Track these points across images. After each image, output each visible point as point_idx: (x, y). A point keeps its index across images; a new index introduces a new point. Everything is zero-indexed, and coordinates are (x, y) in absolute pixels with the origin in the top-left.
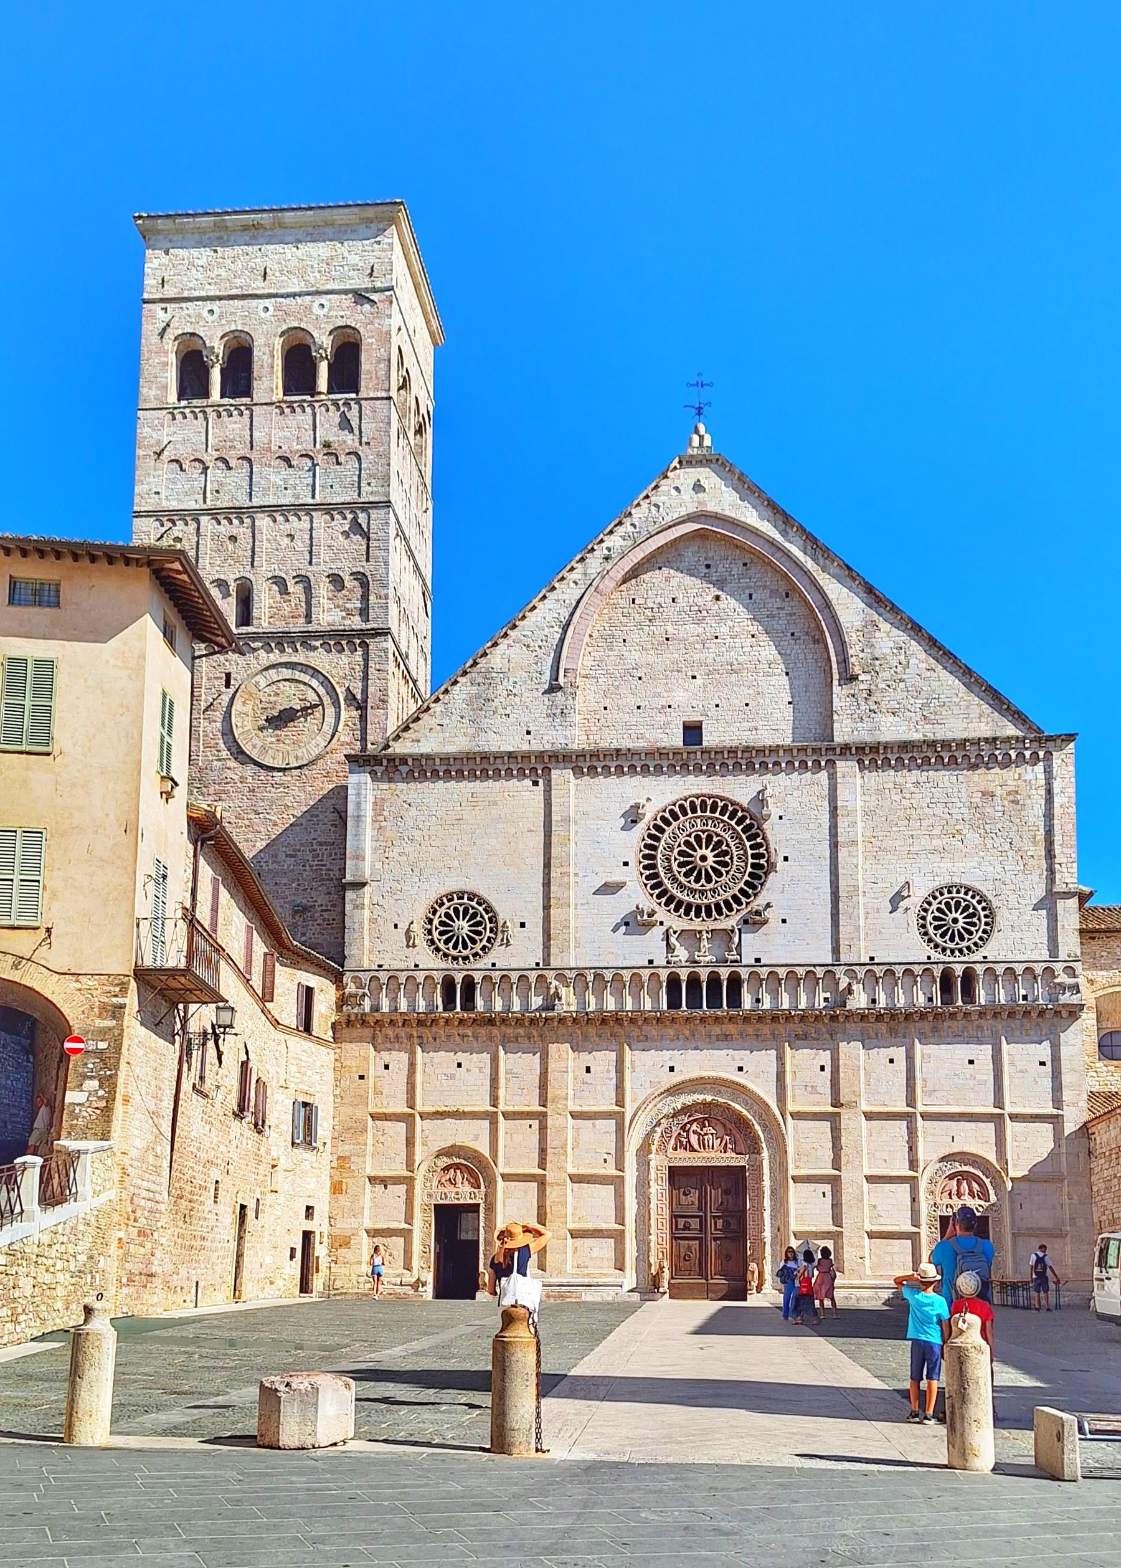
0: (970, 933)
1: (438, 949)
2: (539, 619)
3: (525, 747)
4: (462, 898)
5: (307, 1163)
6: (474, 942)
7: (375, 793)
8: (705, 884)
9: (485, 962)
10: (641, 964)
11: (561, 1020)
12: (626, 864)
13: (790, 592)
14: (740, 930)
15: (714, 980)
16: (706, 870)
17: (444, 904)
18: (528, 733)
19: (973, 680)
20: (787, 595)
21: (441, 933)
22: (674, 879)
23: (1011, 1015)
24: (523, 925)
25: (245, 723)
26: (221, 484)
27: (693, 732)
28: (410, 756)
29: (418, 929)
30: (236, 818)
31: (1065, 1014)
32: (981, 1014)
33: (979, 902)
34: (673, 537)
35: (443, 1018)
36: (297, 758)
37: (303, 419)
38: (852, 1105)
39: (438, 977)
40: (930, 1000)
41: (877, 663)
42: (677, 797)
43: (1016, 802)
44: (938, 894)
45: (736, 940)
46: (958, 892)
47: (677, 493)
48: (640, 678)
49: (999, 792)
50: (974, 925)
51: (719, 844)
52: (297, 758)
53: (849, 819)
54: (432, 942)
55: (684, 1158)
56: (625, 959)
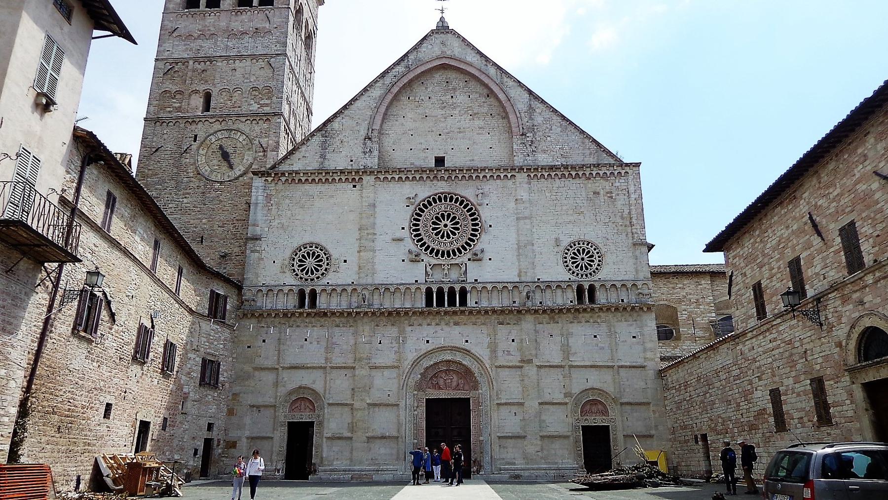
0: (591, 266)
1: (297, 275)
2: (359, 105)
3: (350, 168)
4: (312, 247)
5: (210, 397)
6: (317, 270)
7: (267, 191)
8: (447, 239)
9: (324, 281)
10: (411, 282)
11: (366, 313)
12: (403, 228)
13: (491, 94)
14: (466, 264)
15: (452, 291)
16: (447, 233)
17: (301, 250)
18: (352, 161)
19: (585, 136)
20: (488, 96)
21: (299, 266)
22: (429, 236)
23: (617, 309)
24: (345, 261)
25: (202, 159)
26: (201, 46)
27: (440, 161)
28: (287, 171)
29: (286, 262)
30: (194, 207)
31: (645, 309)
32: (601, 309)
33: (595, 249)
34: (429, 67)
35: (297, 312)
36: (229, 176)
37: (244, 17)
38: (530, 361)
39: (295, 289)
40: (571, 302)
41: (536, 128)
42: (431, 194)
43: (612, 197)
44: (572, 245)
45: (464, 269)
46: (583, 244)
47: (432, 47)
48: (412, 135)
49: (602, 192)
50: (593, 261)
51: (454, 218)
52: (229, 176)
53: (524, 205)
54: (294, 271)
55: (435, 394)
56: (402, 280)
